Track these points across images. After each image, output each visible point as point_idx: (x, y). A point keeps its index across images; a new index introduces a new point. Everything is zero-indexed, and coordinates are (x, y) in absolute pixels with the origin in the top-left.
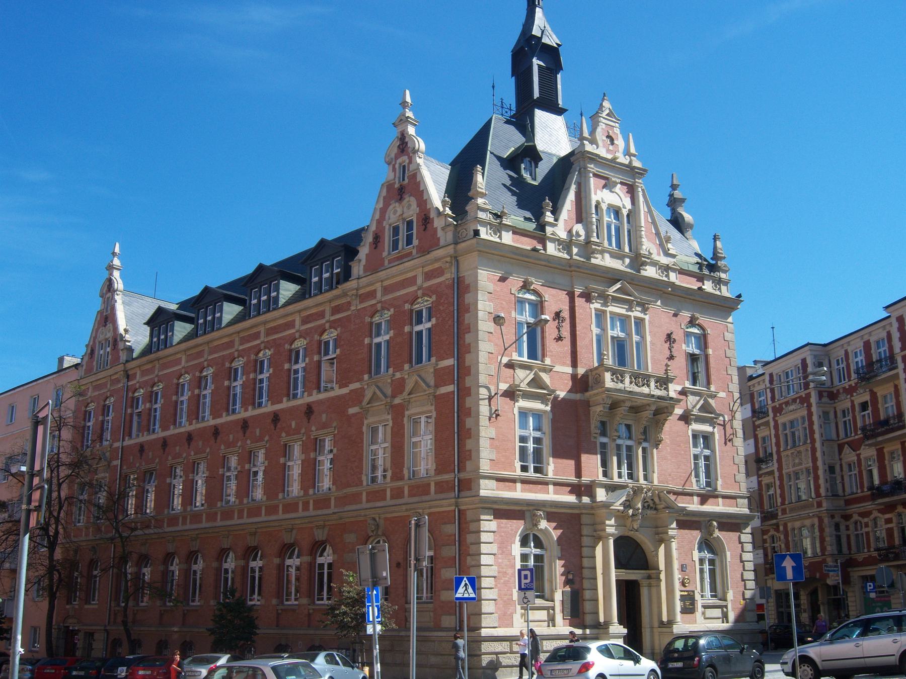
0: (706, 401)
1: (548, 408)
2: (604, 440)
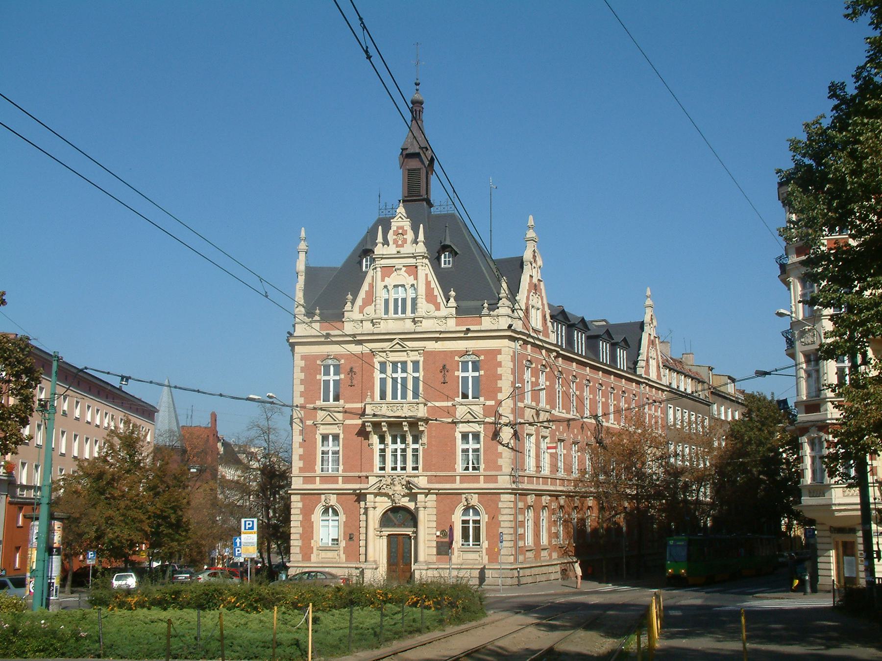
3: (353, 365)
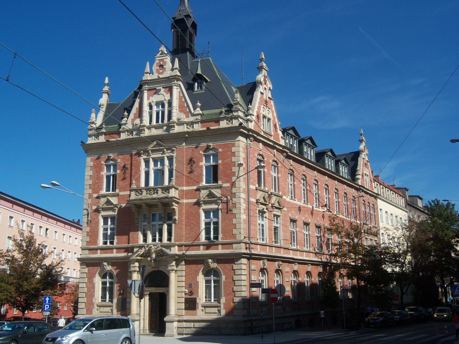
0: (210, 191)
1: (116, 213)
3: (127, 162)
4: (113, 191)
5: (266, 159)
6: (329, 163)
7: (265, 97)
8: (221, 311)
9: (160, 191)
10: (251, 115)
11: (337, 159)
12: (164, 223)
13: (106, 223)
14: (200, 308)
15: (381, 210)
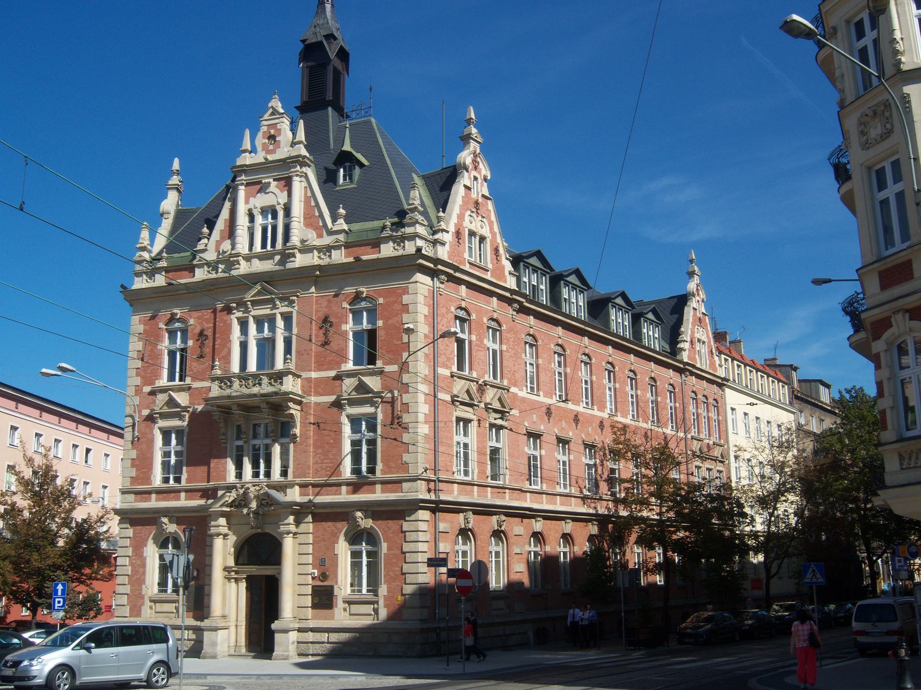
0: (360, 380)
1: (185, 423)
2: (240, 443)
3: (206, 325)
4: (181, 380)
5: (474, 317)
6: (619, 321)
7: (474, 195)
8: (380, 611)
9: (265, 380)
10: (443, 230)
11: (635, 311)
12: (275, 441)
13: (166, 442)
14: (340, 604)
15: (733, 409)
